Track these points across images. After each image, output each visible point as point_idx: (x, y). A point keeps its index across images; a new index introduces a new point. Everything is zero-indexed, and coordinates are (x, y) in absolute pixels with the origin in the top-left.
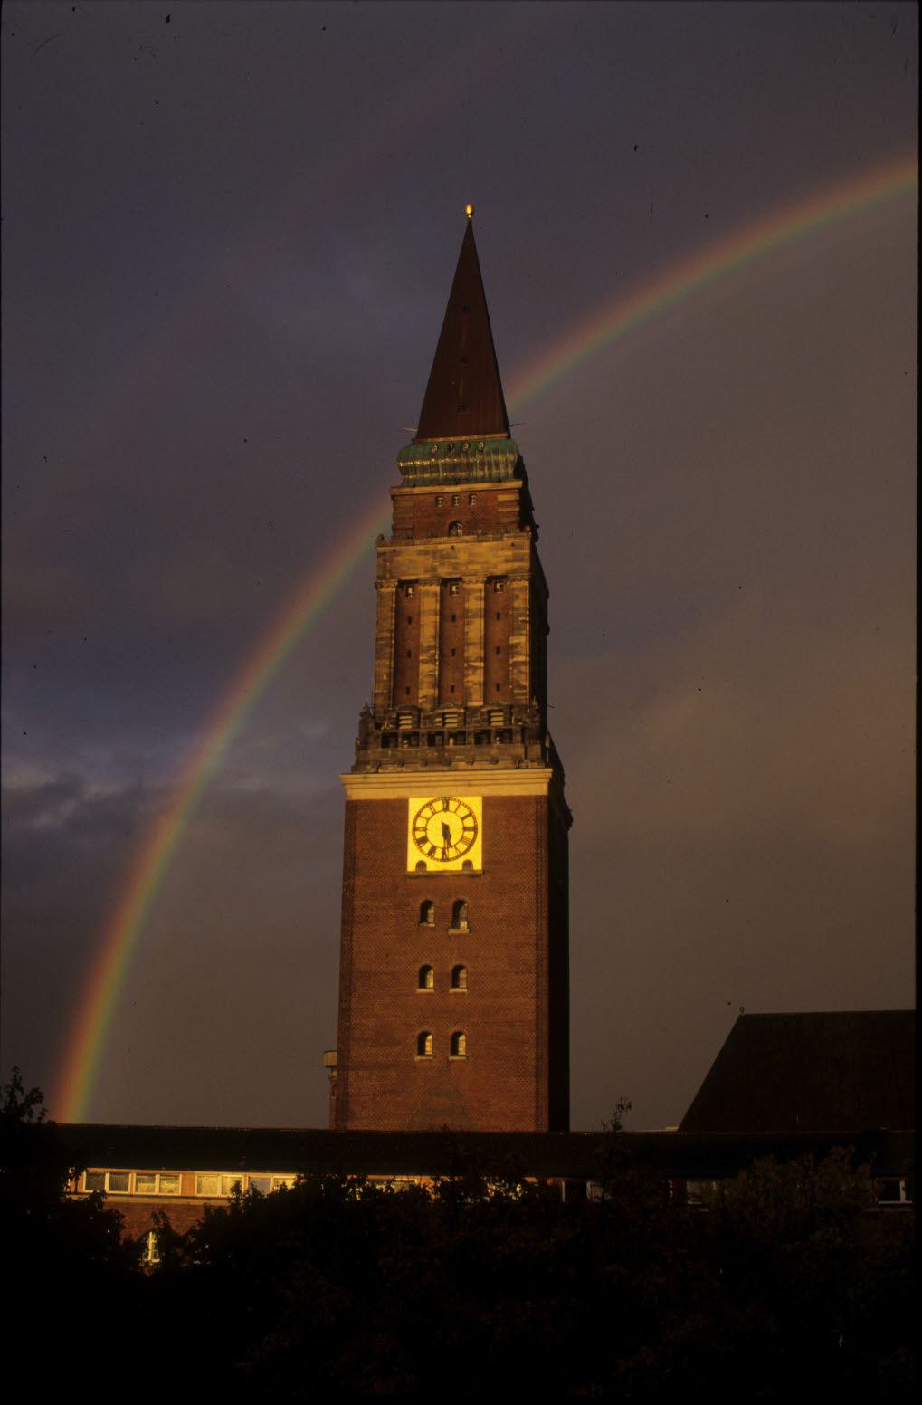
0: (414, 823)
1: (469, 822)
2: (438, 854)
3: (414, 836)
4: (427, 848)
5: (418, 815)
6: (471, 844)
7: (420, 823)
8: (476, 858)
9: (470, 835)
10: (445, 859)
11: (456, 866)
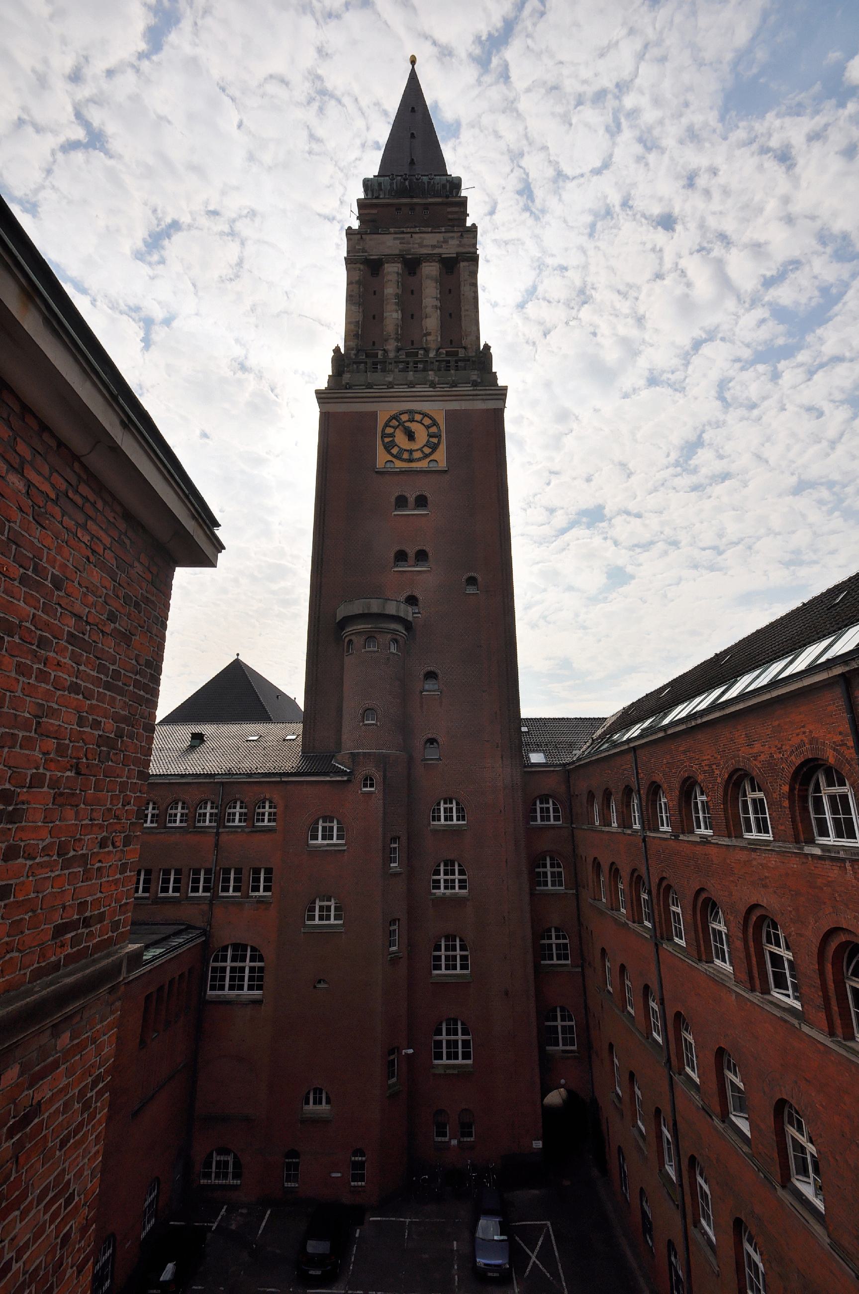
0: (383, 430)
1: (434, 430)
3: (383, 441)
4: (395, 451)
5: (387, 425)
6: (434, 448)
7: (389, 430)
8: (441, 456)
9: (435, 440)
10: (411, 460)
11: (423, 465)
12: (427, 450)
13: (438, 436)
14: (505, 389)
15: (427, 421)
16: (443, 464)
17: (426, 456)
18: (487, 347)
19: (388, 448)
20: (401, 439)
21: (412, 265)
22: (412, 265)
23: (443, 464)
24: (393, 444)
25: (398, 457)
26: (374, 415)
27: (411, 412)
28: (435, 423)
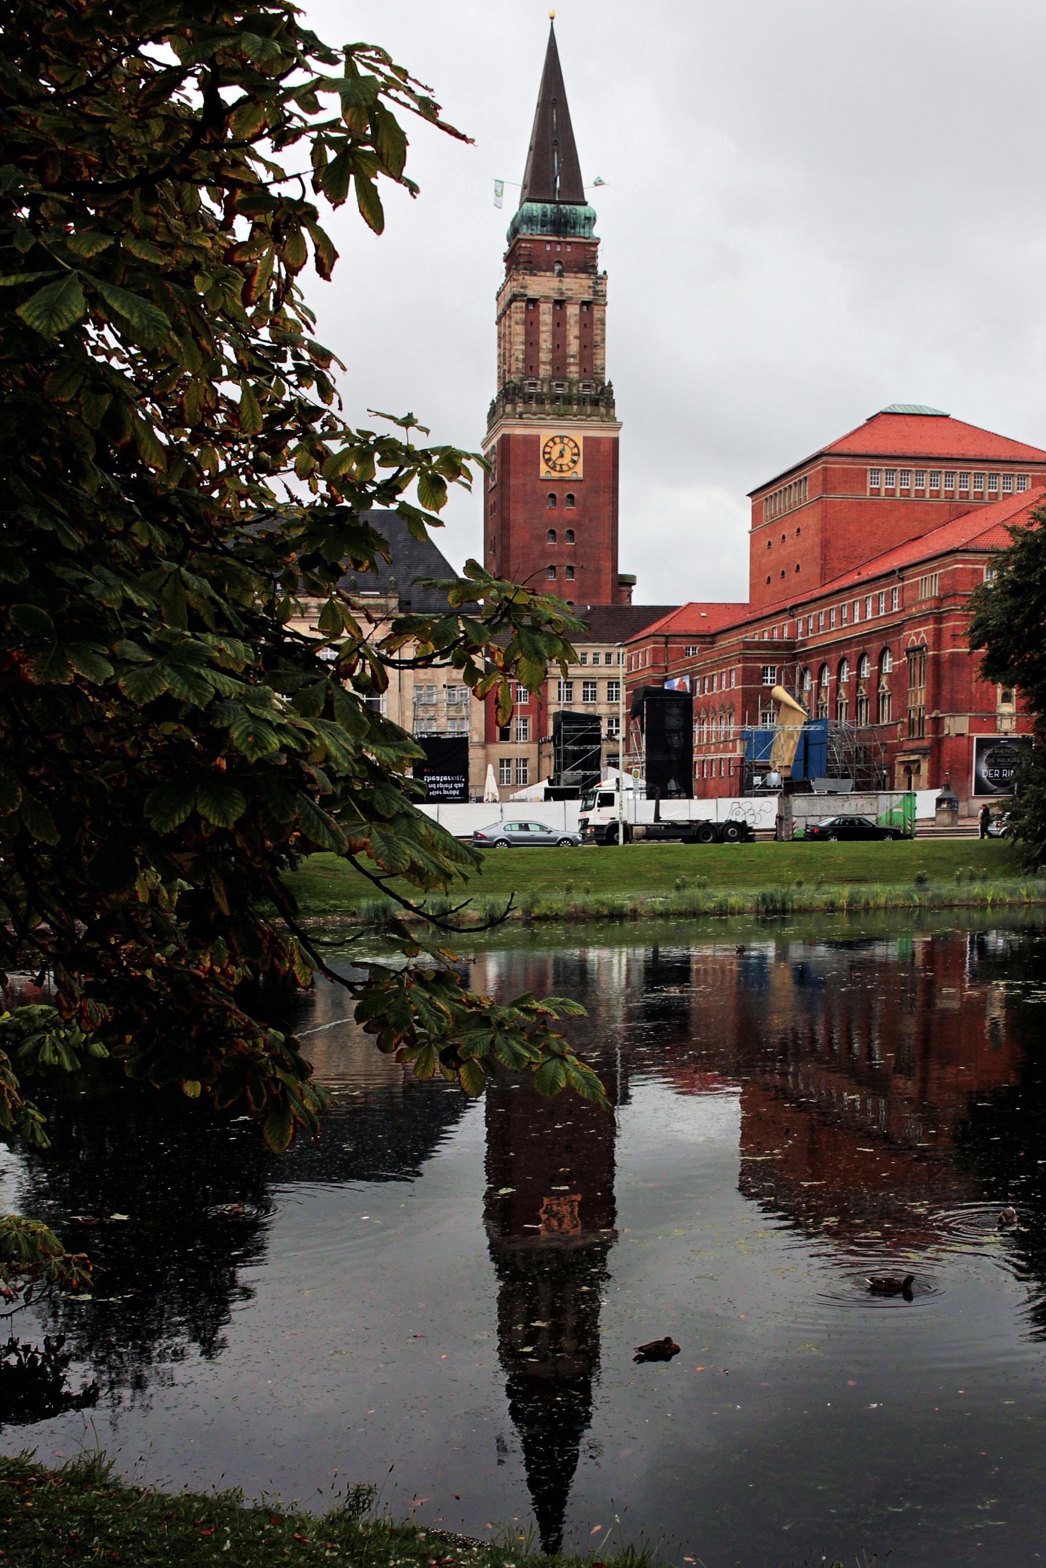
1: (575, 451)
2: (558, 468)
5: (546, 445)
7: (548, 450)
8: (579, 471)
9: (575, 458)
10: (561, 471)
11: (566, 475)
12: (571, 465)
13: (578, 455)
14: (621, 424)
15: (572, 445)
16: (581, 476)
17: (570, 469)
18: (610, 383)
19: (547, 461)
20: (555, 455)
21: (560, 303)
22: (560, 303)
23: (581, 476)
24: (549, 460)
25: (553, 468)
26: (538, 437)
27: (562, 437)
28: (576, 446)
